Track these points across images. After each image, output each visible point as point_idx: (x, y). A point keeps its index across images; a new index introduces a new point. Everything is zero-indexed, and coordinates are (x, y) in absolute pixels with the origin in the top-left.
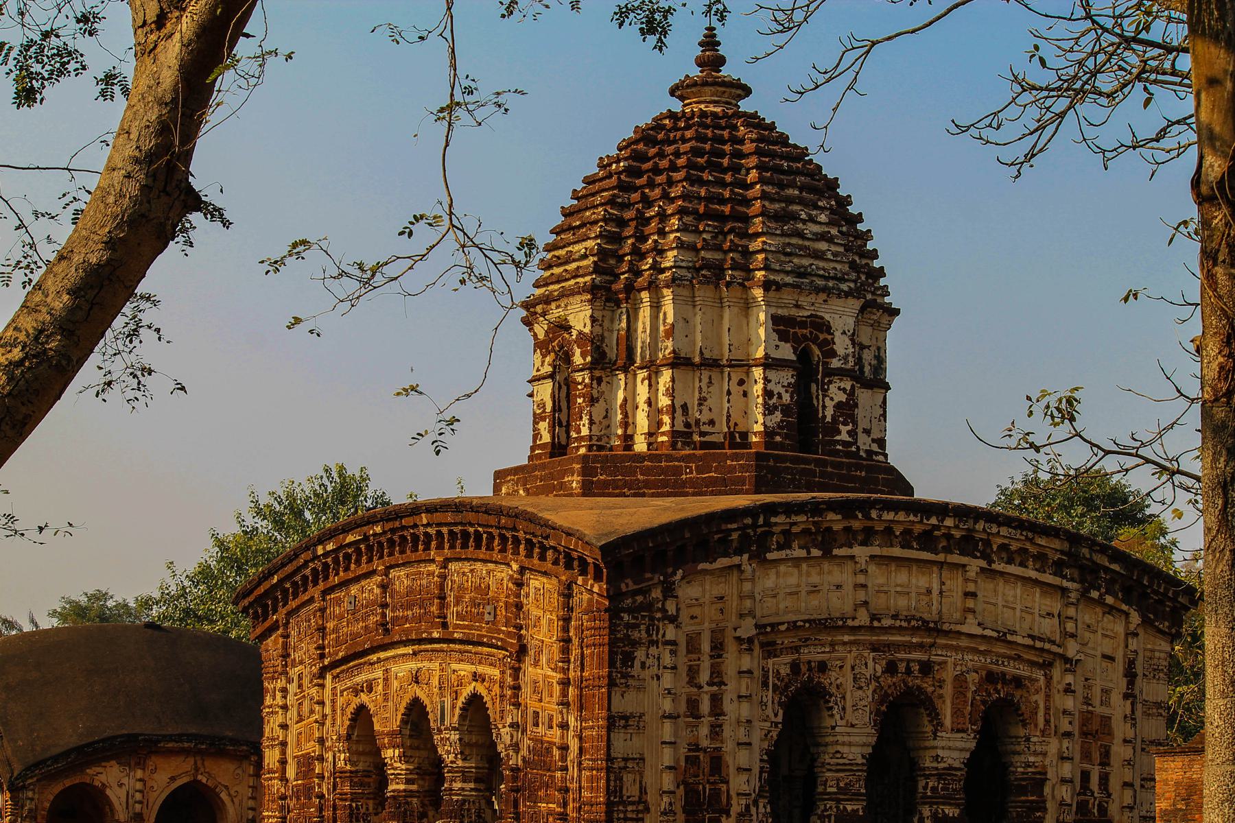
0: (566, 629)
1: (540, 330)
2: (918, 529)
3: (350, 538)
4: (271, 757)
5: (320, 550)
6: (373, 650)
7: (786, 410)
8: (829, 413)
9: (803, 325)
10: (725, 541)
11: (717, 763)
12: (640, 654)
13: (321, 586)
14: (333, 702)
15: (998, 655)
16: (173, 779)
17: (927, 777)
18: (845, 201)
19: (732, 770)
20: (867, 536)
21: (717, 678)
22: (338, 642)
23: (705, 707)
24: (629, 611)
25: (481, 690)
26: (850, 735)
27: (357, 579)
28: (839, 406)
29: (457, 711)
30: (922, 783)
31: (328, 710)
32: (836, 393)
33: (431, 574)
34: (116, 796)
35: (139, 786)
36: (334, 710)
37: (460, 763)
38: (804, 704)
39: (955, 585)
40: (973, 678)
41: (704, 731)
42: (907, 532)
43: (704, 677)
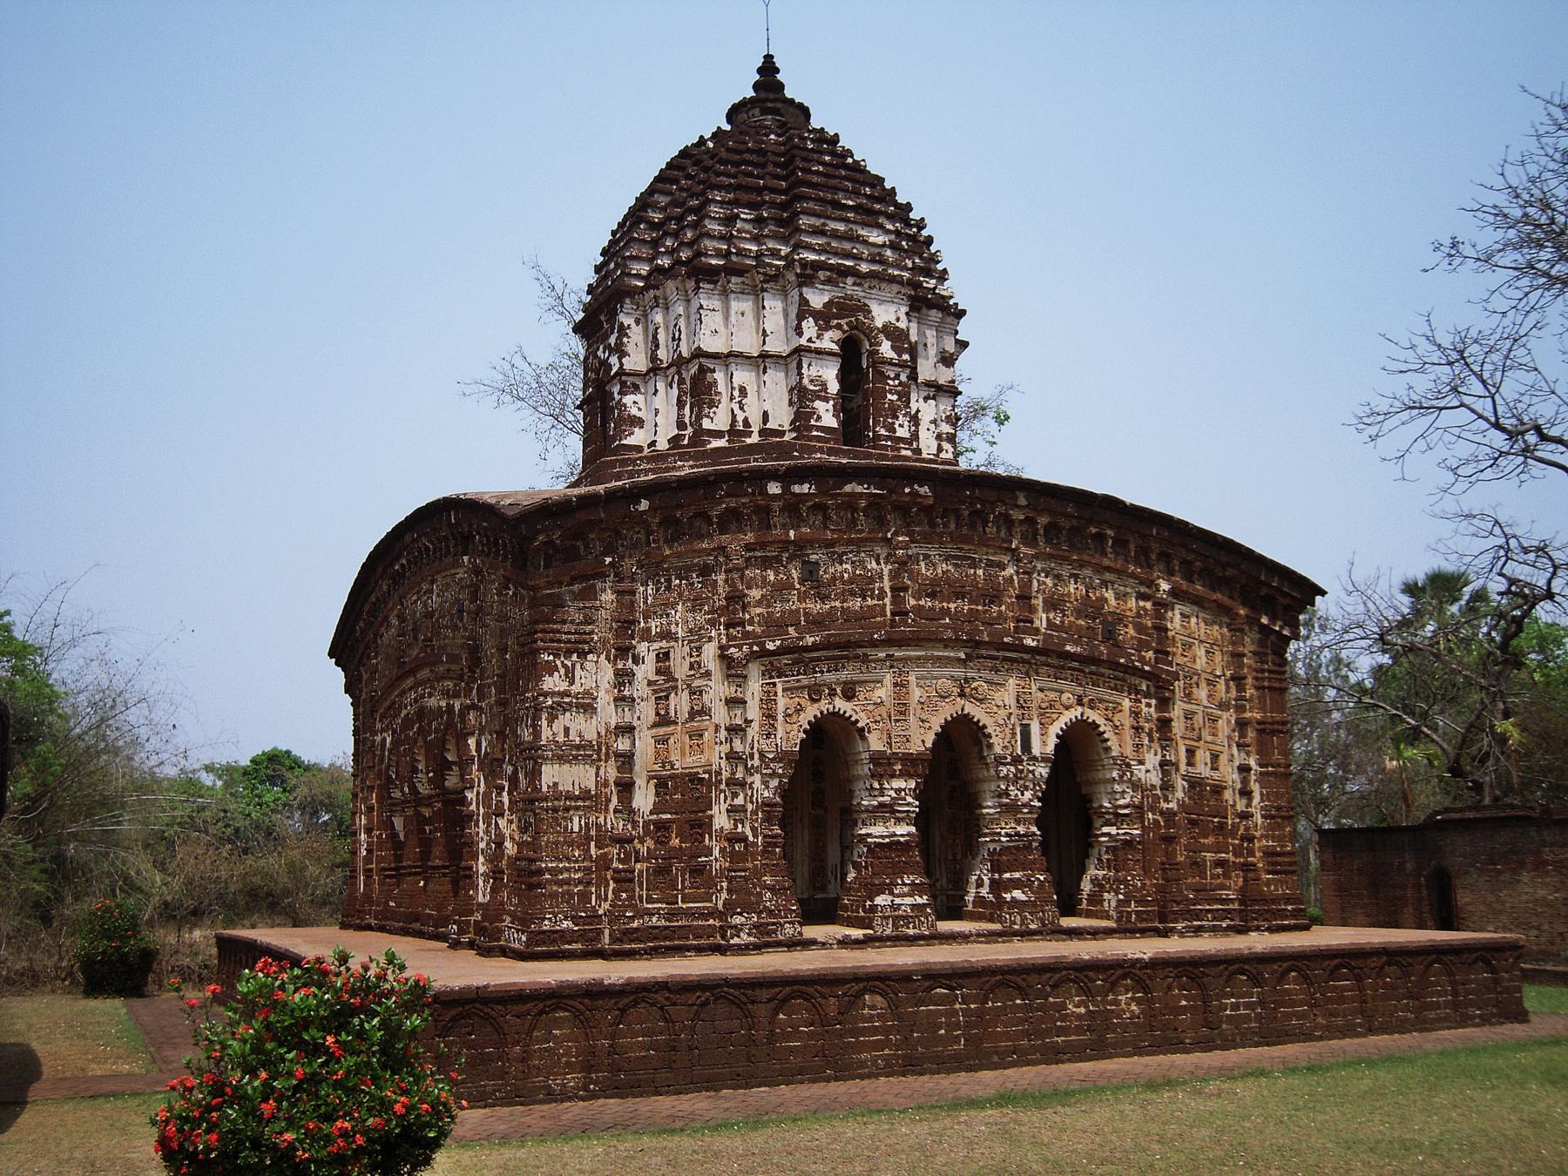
6: (874, 644)
29: (1052, 741)
31: (754, 712)
36: (770, 716)
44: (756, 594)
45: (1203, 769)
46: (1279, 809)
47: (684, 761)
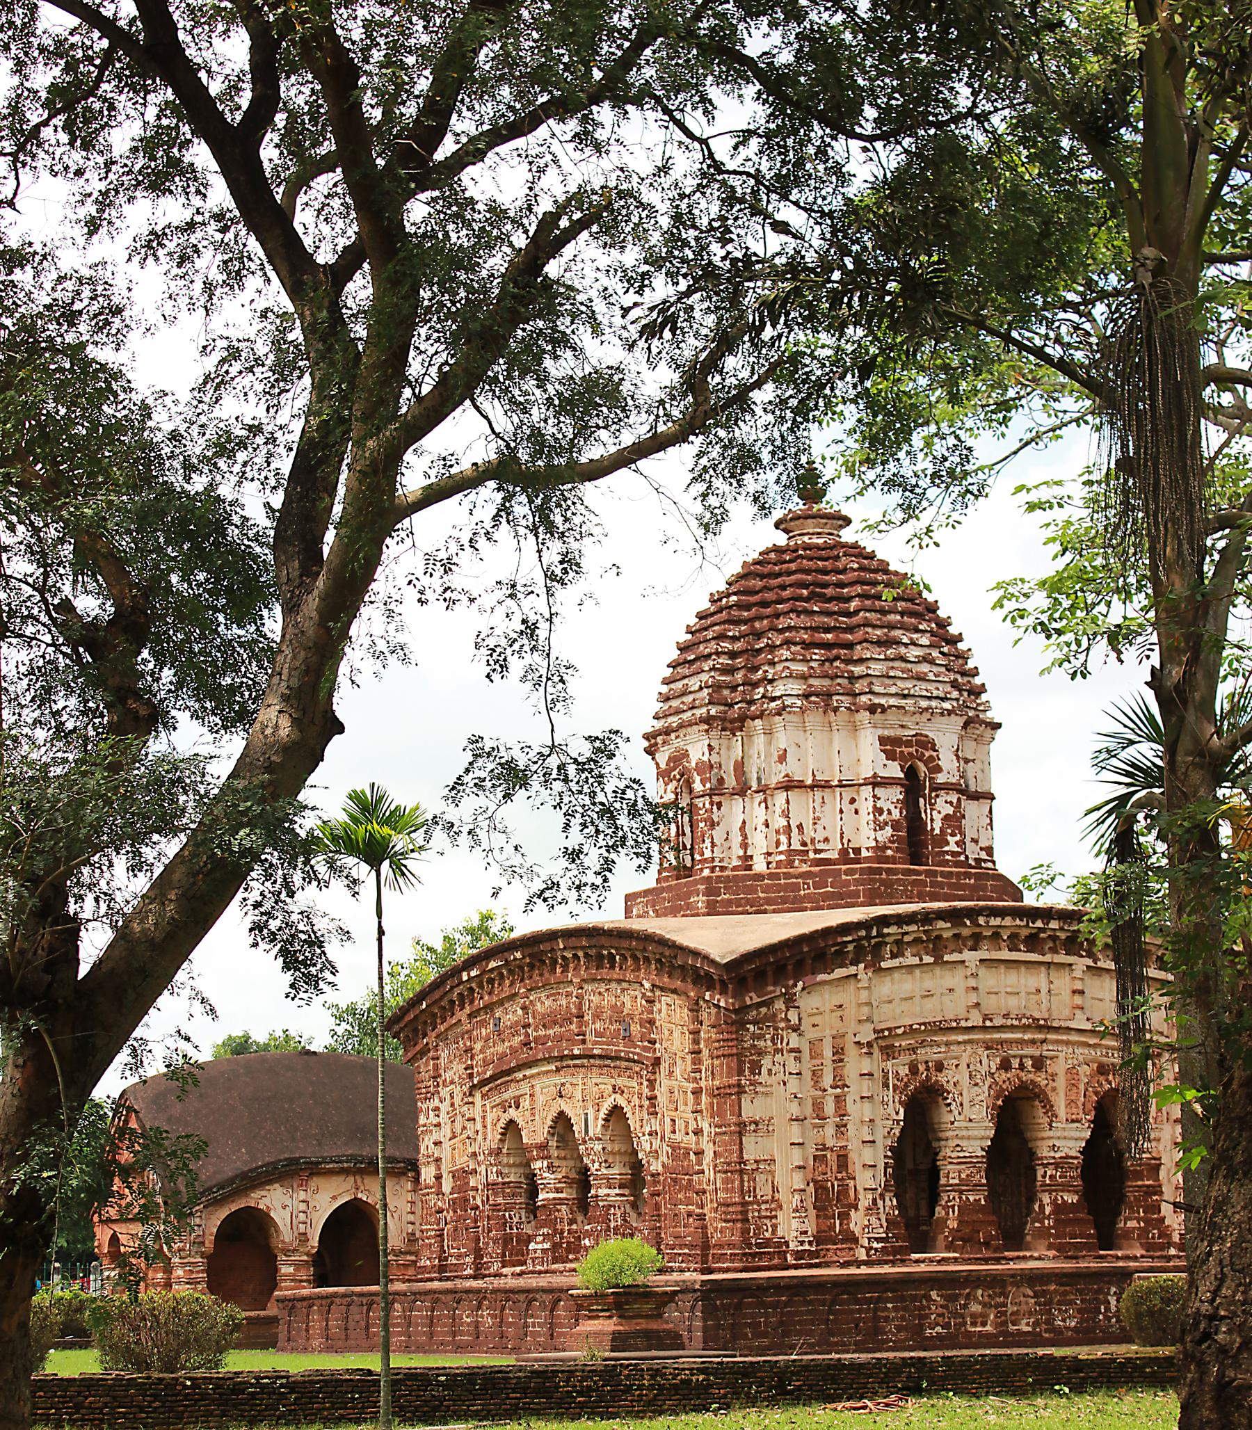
0: (696, 1042)
1: (663, 757)
2: (1024, 933)
3: (492, 964)
4: (427, 1174)
5: (465, 977)
6: (519, 1067)
7: (896, 825)
8: (937, 825)
9: (908, 744)
10: (840, 953)
11: (843, 1160)
12: (766, 1062)
13: (467, 1010)
14: (484, 1117)
15: (1108, 1047)
16: (334, 1198)
17: (1045, 1166)
18: (943, 624)
19: (858, 1167)
20: (976, 941)
21: (840, 1082)
22: (486, 1064)
23: (830, 1108)
24: (755, 1023)
25: (621, 1101)
26: (967, 1130)
27: (501, 1003)
28: (946, 818)
29: (601, 1122)
30: (1040, 1172)
31: (479, 1126)
32: (943, 806)
33: (568, 995)
34: (280, 1217)
35: (303, 1206)
37: (604, 1171)
38: (923, 1105)
39: (1063, 983)
40: (1085, 1070)
41: (830, 1130)
42: (1013, 937)
43: (827, 1080)
44: (478, 1046)
45: (678, 1137)
46: (728, 1164)
47: (463, 1161)
